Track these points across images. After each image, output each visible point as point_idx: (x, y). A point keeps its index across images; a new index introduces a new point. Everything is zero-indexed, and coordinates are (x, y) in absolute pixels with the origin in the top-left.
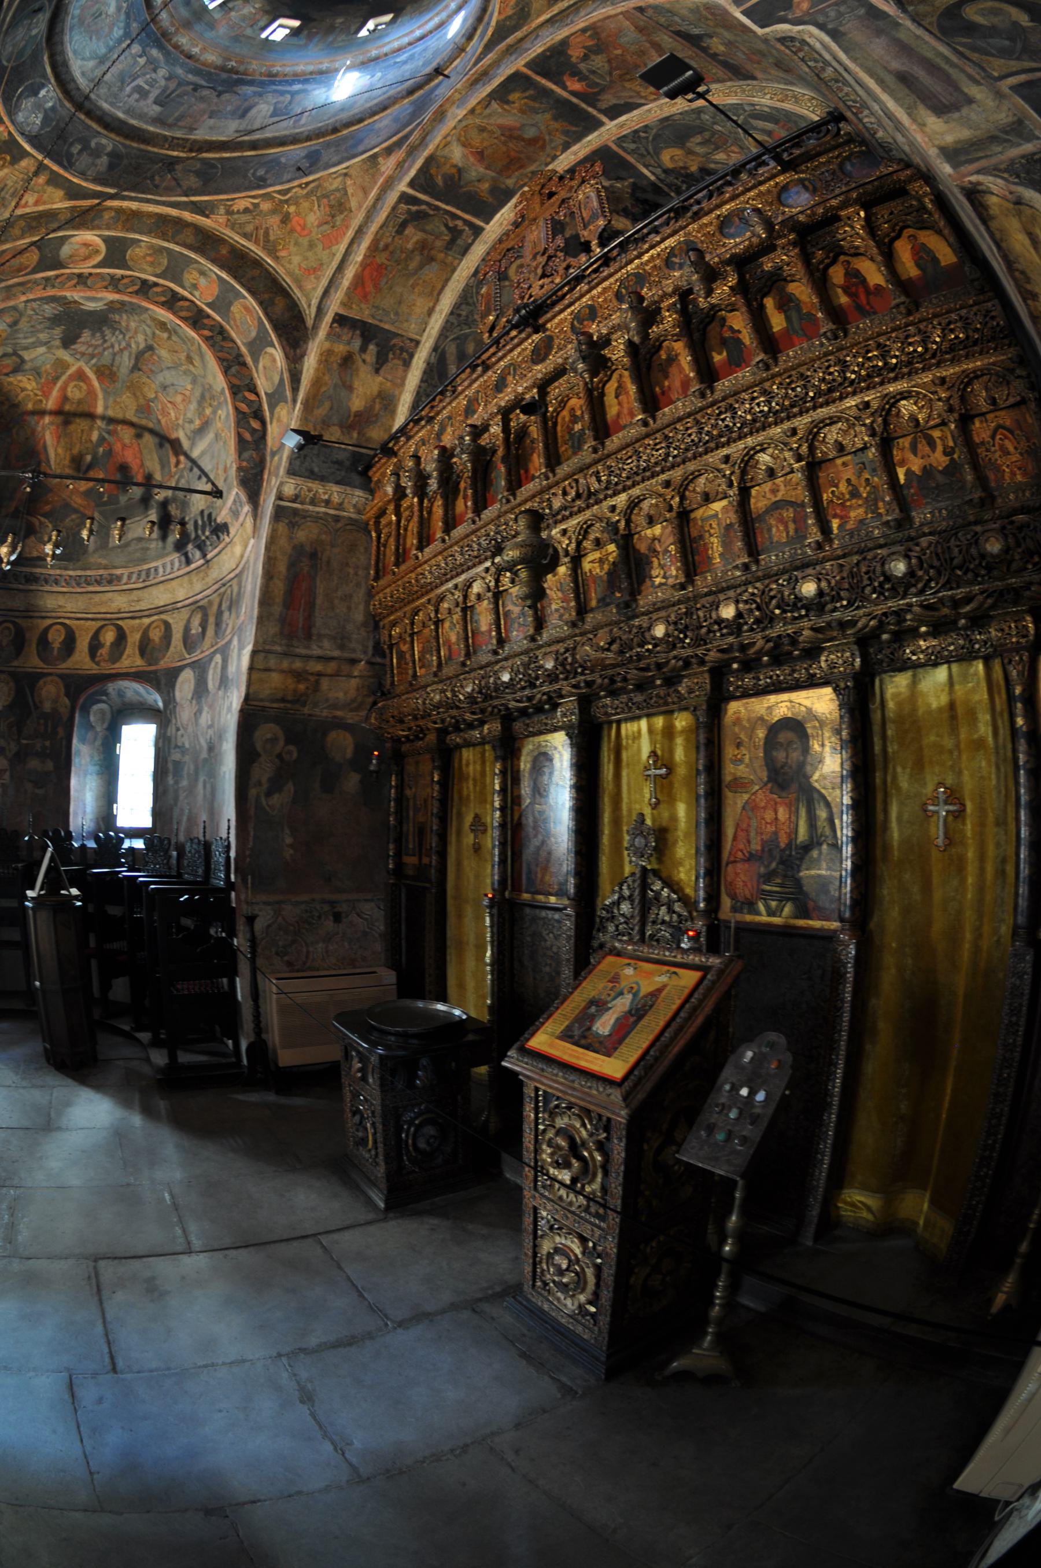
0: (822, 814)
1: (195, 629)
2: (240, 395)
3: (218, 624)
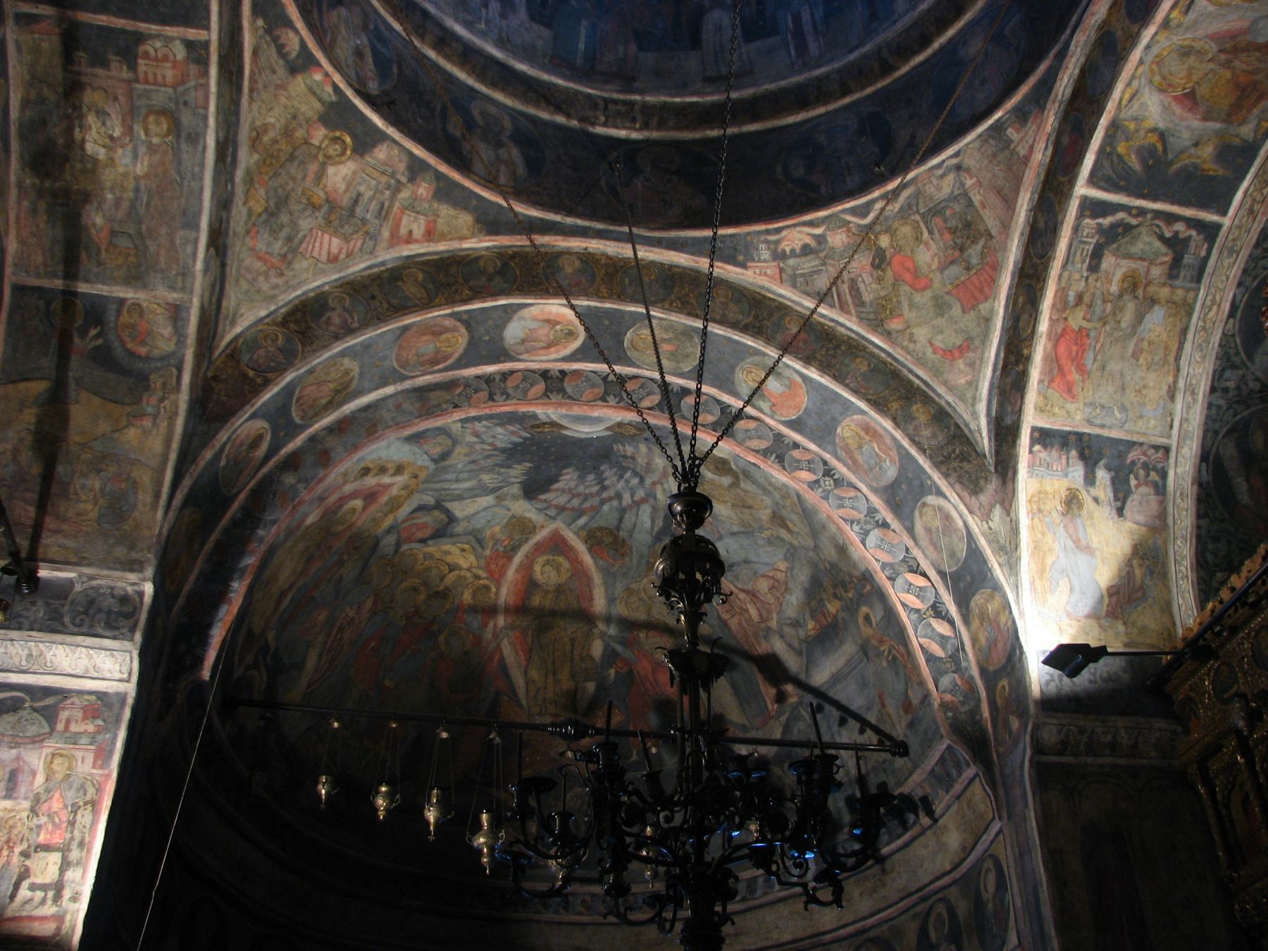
2: (899, 581)
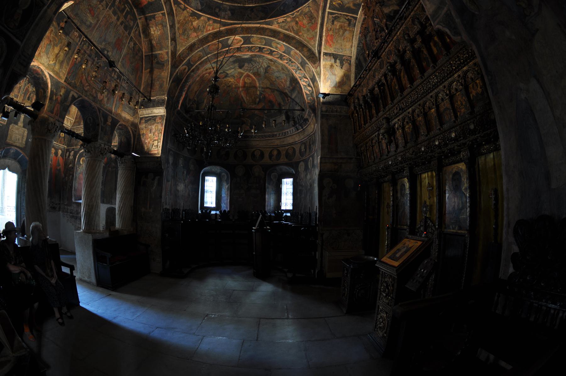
1: (303, 150)
3: (310, 148)
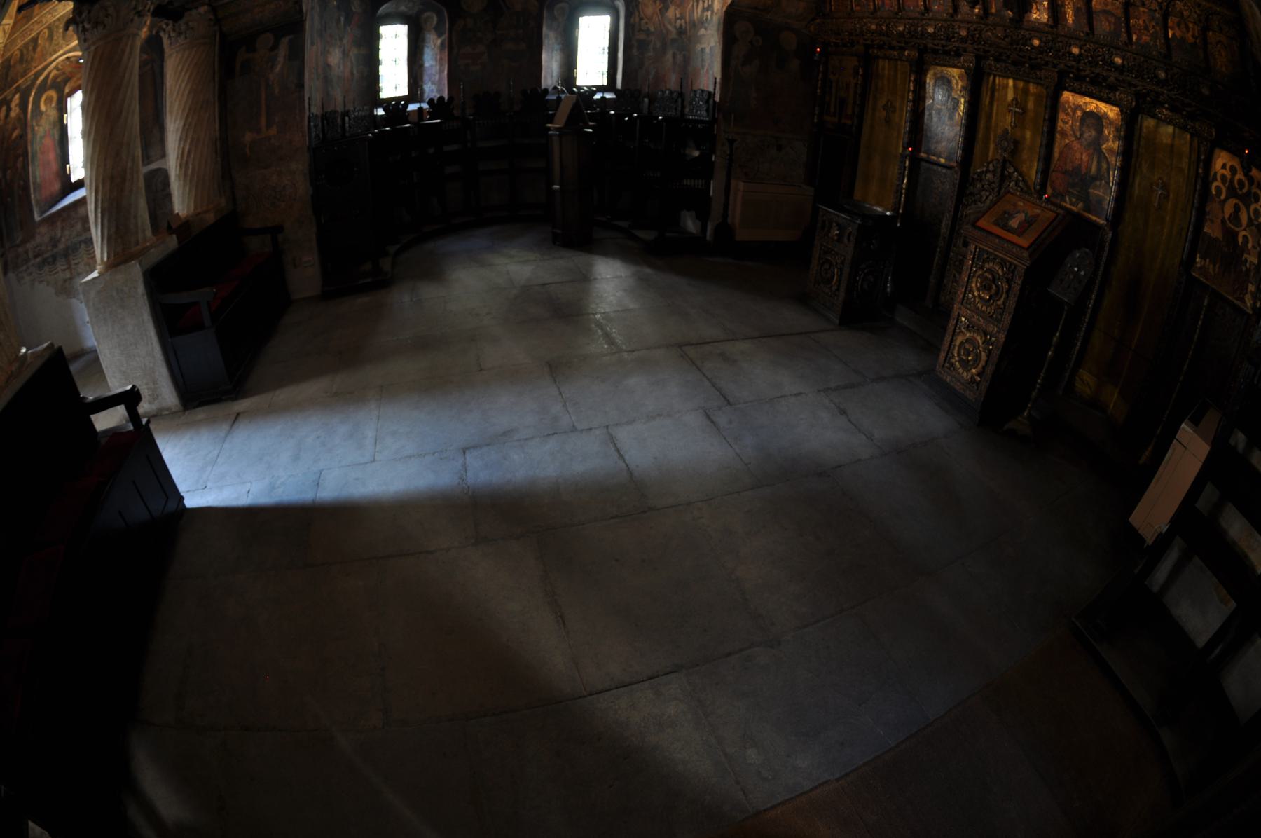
0: (1104, 166)
